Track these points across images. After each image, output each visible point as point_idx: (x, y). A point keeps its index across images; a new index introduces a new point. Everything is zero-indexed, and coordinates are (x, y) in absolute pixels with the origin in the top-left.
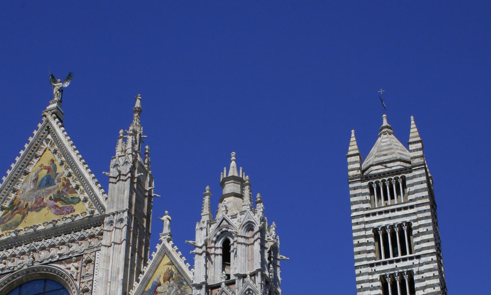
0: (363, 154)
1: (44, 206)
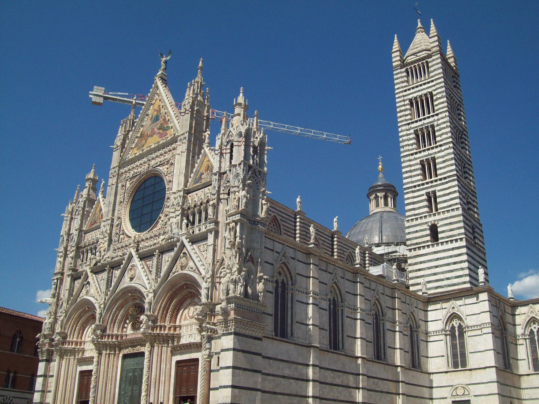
0: (404, 49)
1: (155, 133)
